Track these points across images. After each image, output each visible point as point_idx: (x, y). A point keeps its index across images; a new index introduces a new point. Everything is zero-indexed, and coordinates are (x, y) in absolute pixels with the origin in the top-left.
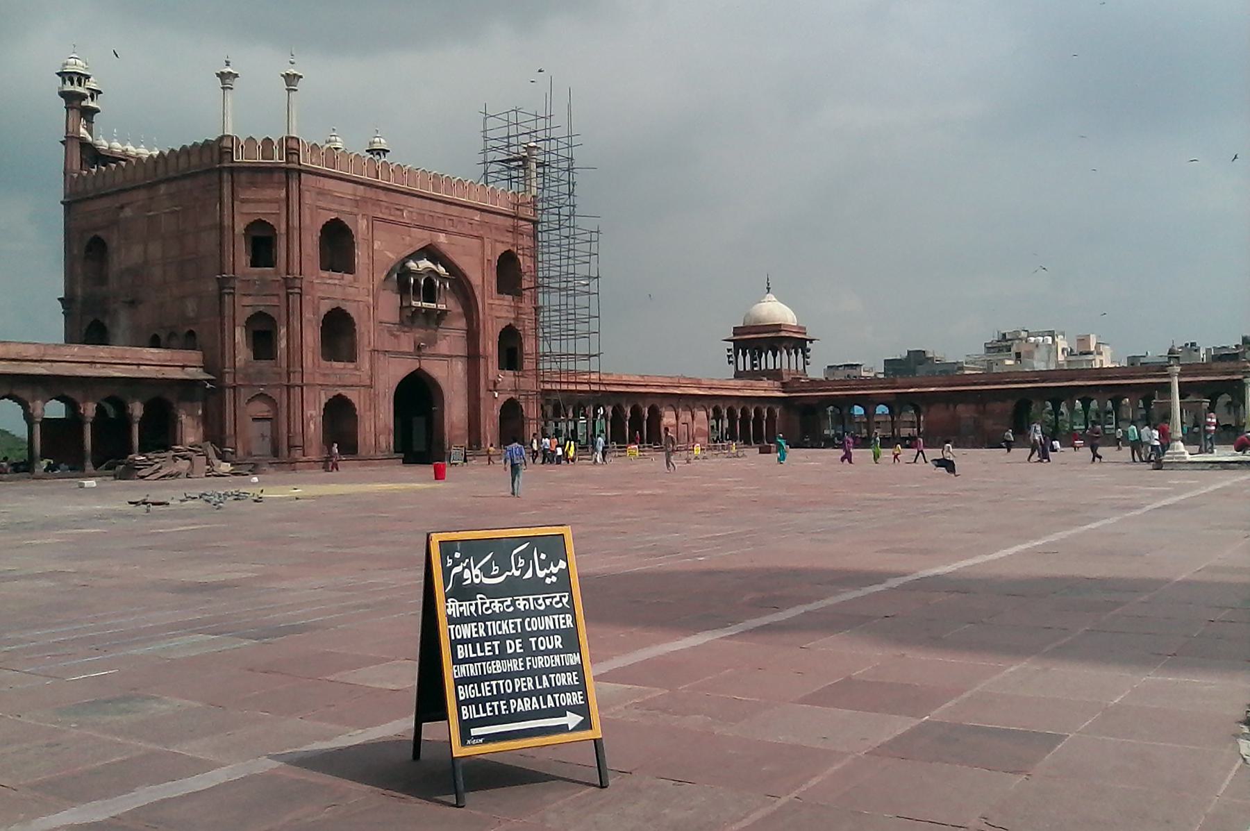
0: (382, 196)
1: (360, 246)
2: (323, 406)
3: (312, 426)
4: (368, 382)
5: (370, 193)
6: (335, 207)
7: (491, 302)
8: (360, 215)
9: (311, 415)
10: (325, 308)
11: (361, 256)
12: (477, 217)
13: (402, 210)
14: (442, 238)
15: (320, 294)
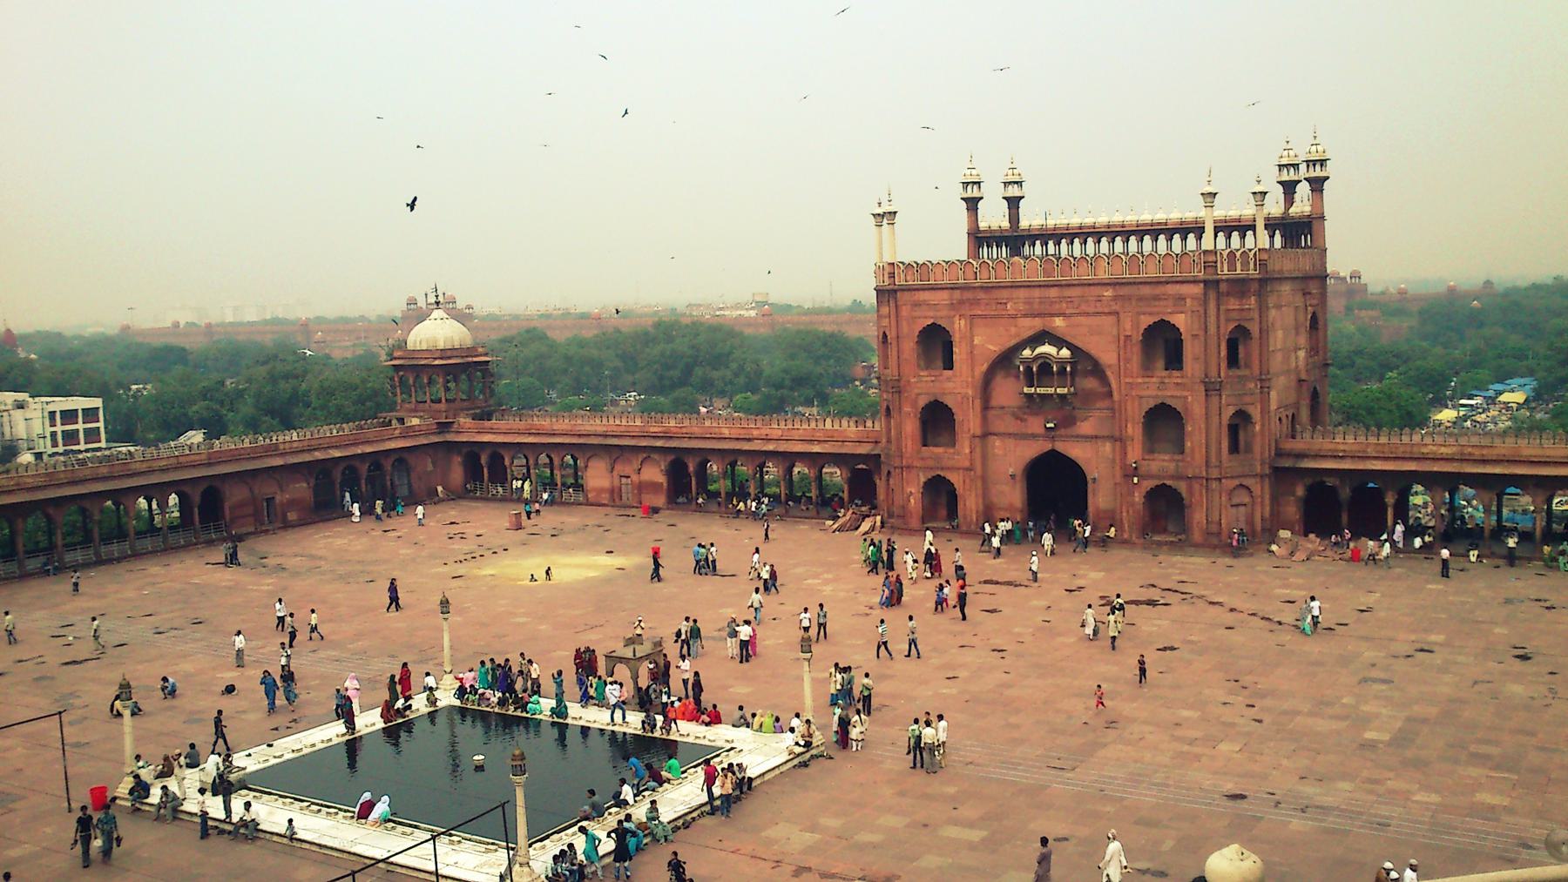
0: (981, 295)
1: (958, 344)
2: (922, 484)
3: (912, 501)
4: (967, 464)
5: (968, 295)
6: (932, 314)
7: (1127, 380)
8: (958, 316)
9: (911, 492)
10: (922, 402)
11: (959, 353)
12: (1109, 293)
13: (1006, 304)
14: (1059, 322)
15: (916, 391)
